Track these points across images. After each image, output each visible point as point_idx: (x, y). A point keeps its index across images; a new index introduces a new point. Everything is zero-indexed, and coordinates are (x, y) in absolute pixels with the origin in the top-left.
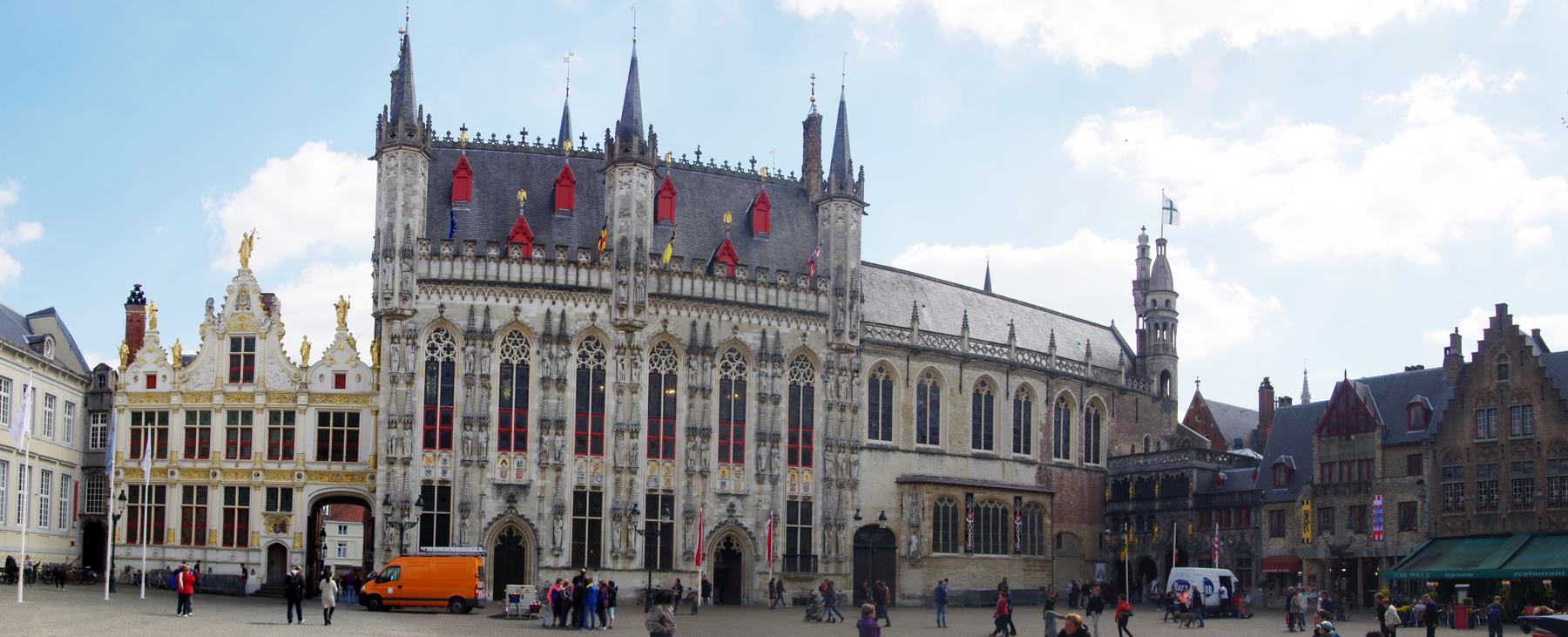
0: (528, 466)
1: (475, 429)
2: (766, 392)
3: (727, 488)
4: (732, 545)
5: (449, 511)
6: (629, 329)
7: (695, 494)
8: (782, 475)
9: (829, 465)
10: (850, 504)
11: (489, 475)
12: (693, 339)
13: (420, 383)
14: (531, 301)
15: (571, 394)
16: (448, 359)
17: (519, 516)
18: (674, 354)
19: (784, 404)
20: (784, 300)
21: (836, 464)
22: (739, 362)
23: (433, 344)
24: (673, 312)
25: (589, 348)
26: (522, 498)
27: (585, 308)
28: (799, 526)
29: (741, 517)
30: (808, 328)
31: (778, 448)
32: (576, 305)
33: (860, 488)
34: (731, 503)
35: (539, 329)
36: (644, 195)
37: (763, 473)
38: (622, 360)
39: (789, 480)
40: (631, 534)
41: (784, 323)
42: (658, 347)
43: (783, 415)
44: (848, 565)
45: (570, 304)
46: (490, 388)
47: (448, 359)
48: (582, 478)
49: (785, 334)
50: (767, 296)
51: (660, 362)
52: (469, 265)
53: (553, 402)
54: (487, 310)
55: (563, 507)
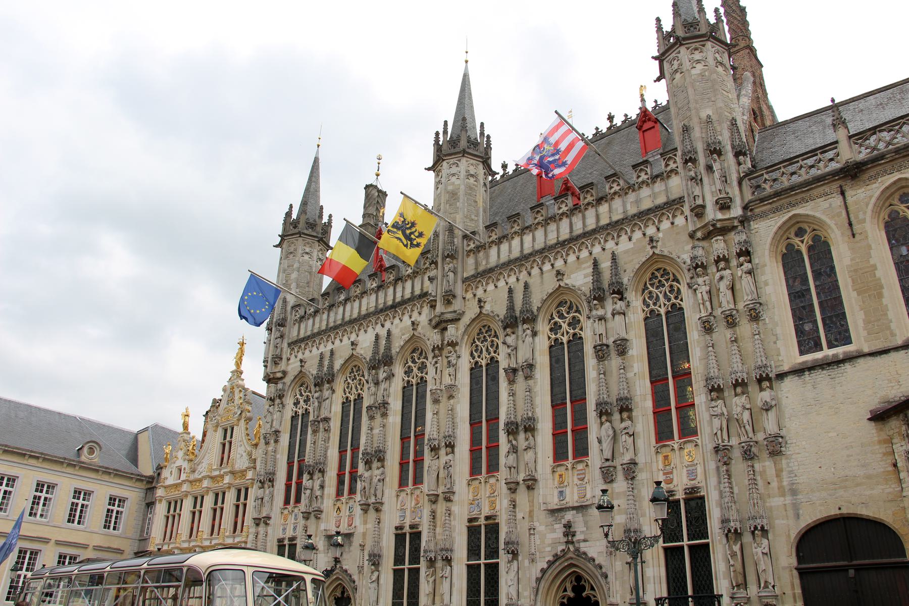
1: (315, 477)
2: (605, 342)
3: (567, 499)
4: (583, 588)
6: (440, 325)
7: (519, 516)
8: (641, 459)
9: (716, 422)
10: (774, 484)
11: (323, 526)
12: (511, 308)
13: (285, 439)
15: (394, 419)
18: (496, 336)
19: (638, 348)
20: (620, 210)
24: (491, 287)
25: (414, 362)
28: (686, 542)
29: (585, 541)
30: (658, 229)
31: (630, 418)
32: (401, 321)
33: (789, 450)
36: (457, 182)
37: (607, 464)
38: (436, 363)
39: (661, 466)
42: (478, 334)
43: (635, 365)
45: (397, 321)
48: (404, 517)
49: (626, 252)
50: (598, 217)
53: (376, 431)
54: (332, 352)
55: (380, 556)
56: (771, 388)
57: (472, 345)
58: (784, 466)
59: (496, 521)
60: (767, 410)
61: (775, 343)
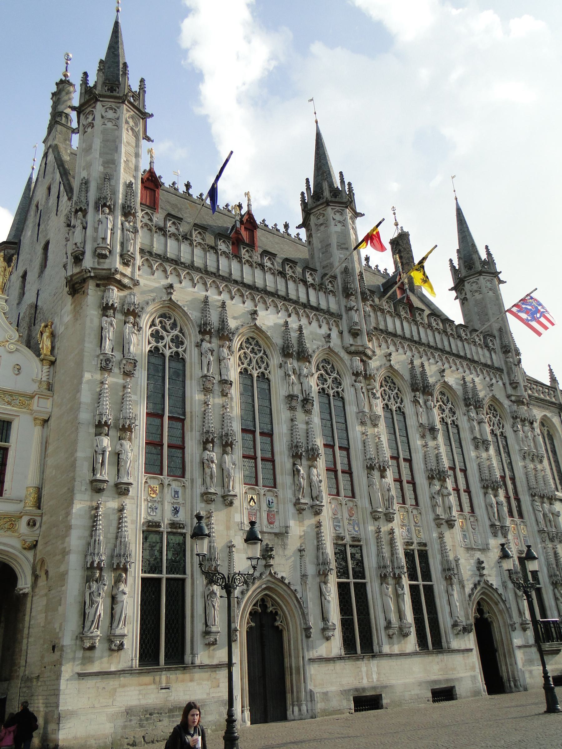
0: (281, 506)
5: (184, 573)
16: (177, 353)
17: (278, 579)
22: (450, 405)
23: (157, 332)
26: (281, 552)
27: (318, 327)
29: (489, 576)
34: (479, 559)
35: (278, 341)
40: (403, 600)
47: (177, 353)
59: (427, 548)
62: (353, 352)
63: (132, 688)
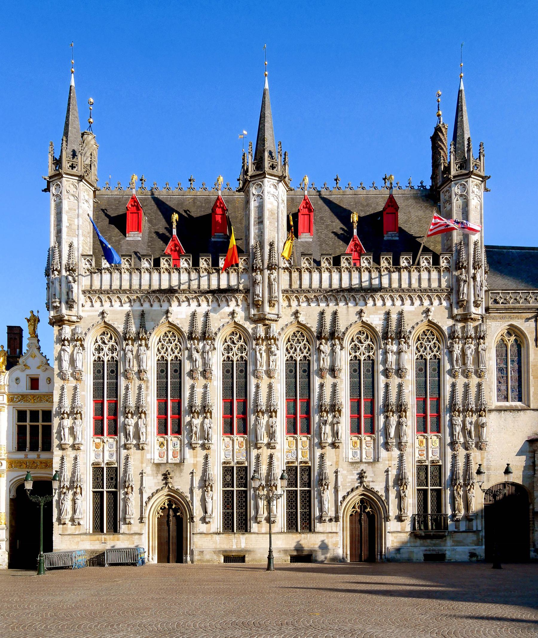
13: (88, 379)
14: (180, 305)
21: (464, 428)
23: (99, 346)
25: (233, 343)
28: (430, 488)
29: (372, 482)
32: (219, 306)
41: (408, 302)
44: (479, 521)
46: (148, 381)
49: (410, 312)
51: (296, 350)
52: (126, 276)
56: (485, 416)
57: (287, 343)
58: (485, 456)
60: (483, 427)
61: (490, 393)
62: (257, 320)
63: (87, 542)
